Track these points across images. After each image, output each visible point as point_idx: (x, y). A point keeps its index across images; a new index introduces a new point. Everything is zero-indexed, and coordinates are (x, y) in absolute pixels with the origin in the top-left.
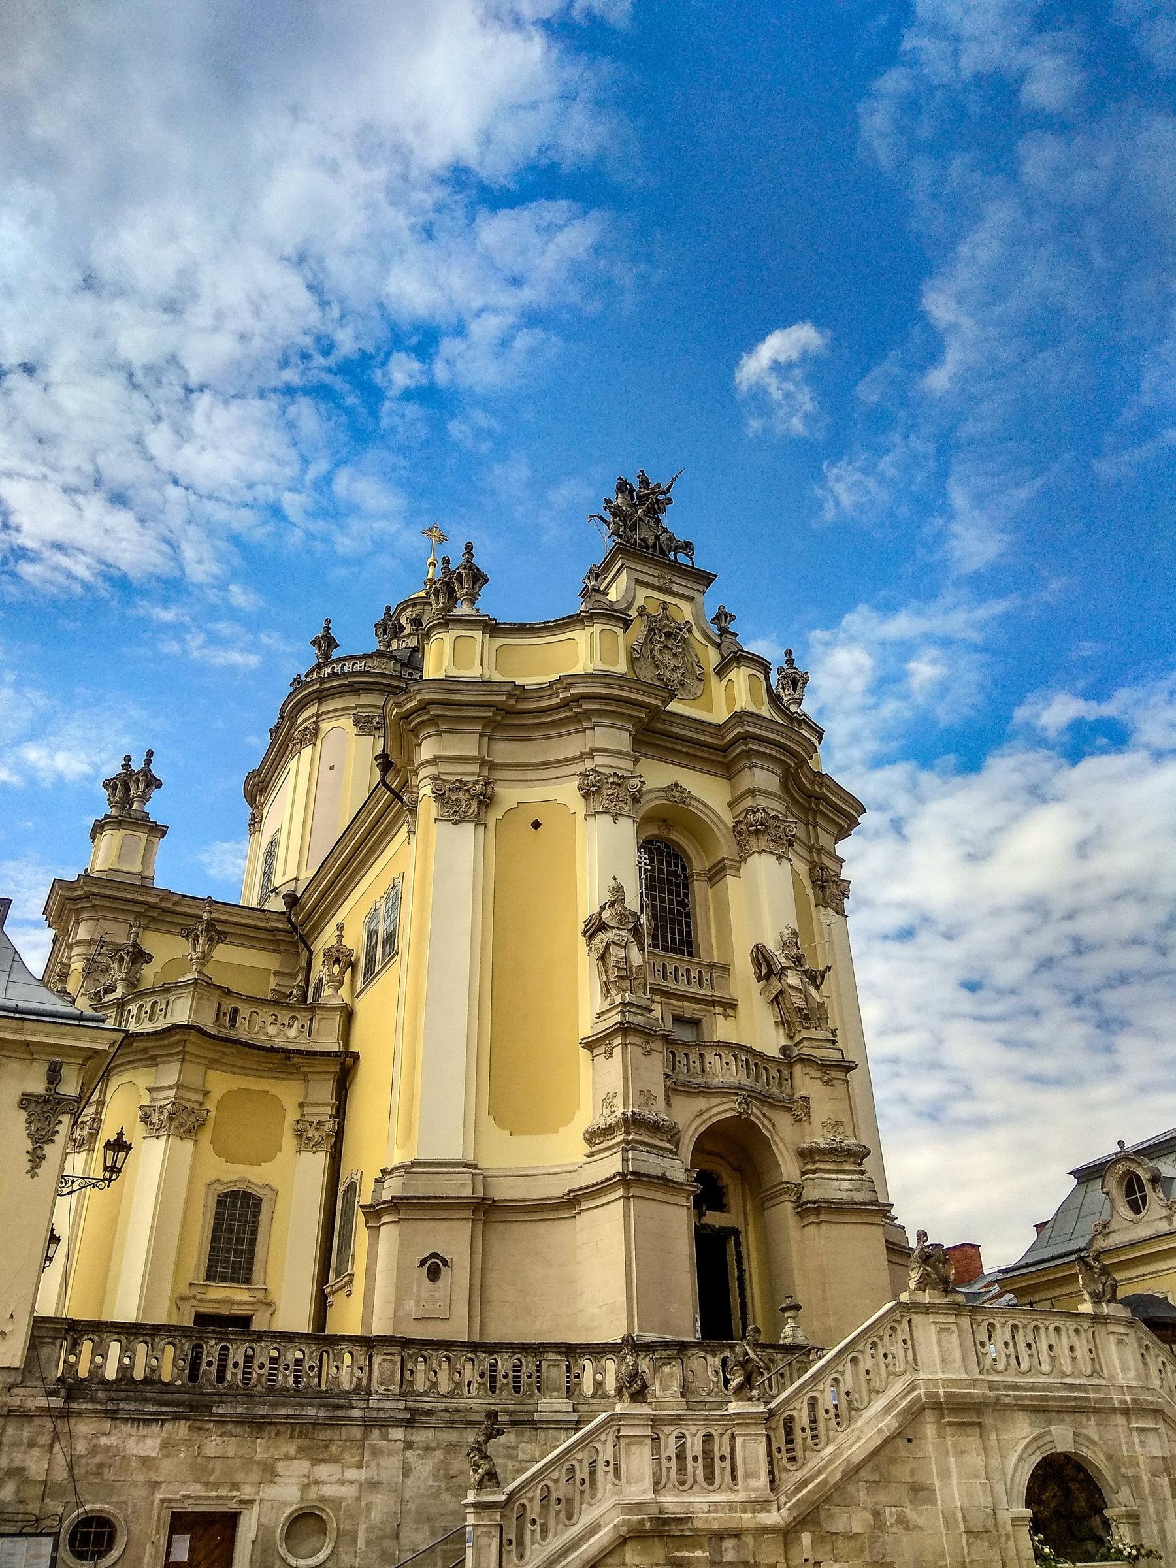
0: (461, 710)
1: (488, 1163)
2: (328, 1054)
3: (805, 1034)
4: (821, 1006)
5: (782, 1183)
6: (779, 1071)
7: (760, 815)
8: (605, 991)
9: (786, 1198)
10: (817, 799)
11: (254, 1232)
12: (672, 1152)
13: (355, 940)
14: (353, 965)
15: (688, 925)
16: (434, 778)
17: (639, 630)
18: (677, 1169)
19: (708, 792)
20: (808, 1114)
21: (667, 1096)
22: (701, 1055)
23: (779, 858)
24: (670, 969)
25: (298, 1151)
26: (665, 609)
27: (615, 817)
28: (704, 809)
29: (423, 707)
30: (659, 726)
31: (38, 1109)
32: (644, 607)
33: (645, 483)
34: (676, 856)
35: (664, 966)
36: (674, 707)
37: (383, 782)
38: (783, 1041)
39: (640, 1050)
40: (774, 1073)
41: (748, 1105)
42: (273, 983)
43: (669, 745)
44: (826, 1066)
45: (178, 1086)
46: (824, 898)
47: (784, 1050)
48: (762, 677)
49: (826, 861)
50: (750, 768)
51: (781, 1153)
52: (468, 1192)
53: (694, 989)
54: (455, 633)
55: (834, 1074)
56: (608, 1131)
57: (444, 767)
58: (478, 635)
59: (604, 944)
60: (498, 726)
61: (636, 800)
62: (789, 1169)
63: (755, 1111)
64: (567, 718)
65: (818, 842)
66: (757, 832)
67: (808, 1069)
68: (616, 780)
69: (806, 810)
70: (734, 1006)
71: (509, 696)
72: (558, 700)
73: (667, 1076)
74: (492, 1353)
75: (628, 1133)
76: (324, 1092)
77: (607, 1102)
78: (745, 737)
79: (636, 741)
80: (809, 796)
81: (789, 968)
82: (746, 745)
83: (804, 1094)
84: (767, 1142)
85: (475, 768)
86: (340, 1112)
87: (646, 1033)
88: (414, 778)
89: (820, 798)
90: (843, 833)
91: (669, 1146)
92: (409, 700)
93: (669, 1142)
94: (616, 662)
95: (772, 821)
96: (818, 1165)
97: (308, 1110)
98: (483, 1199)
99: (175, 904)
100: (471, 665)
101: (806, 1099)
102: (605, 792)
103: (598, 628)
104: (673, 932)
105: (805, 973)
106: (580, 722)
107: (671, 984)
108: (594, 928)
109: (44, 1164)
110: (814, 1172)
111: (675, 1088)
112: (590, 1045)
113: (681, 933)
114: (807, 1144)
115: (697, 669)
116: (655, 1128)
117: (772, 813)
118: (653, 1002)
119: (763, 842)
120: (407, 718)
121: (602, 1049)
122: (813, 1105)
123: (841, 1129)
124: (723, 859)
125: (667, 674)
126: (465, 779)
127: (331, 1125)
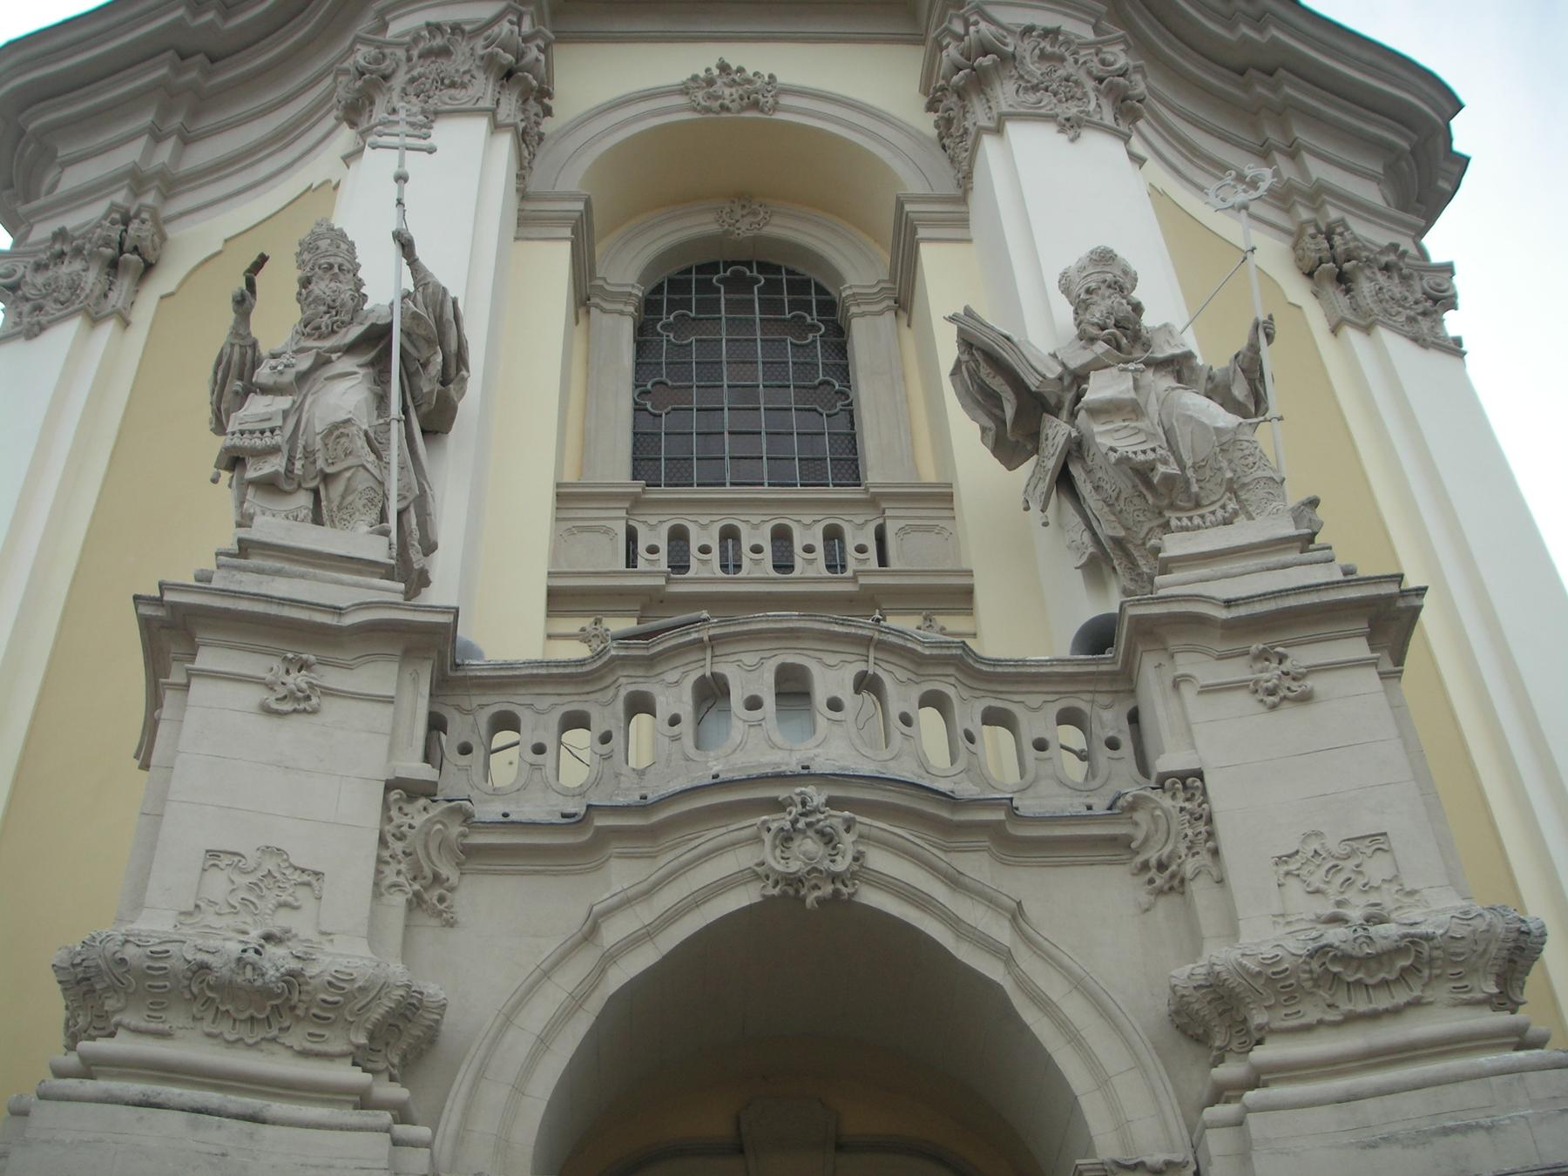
3: (1174, 545)
10: (1271, 74)
12: (364, 1100)
23: (1072, 126)
34: (800, 285)
39: (256, 695)
41: (828, 839)
44: (1269, 626)
46: (1355, 309)
47: (1097, 637)
51: (1075, 1039)
55: (1302, 657)
60: (203, 102)
66: (979, 82)
67: (1186, 663)
68: (439, 41)
69: (1250, 114)
83: (1169, 760)
91: (354, 1076)
93: (358, 1058)
101: (1190, 781)
102: (399, 81)
110: (1256, 1080)
114: (1185, 972)
122: (1221, 795)
123: (1377, 869)
124: (900, 205)
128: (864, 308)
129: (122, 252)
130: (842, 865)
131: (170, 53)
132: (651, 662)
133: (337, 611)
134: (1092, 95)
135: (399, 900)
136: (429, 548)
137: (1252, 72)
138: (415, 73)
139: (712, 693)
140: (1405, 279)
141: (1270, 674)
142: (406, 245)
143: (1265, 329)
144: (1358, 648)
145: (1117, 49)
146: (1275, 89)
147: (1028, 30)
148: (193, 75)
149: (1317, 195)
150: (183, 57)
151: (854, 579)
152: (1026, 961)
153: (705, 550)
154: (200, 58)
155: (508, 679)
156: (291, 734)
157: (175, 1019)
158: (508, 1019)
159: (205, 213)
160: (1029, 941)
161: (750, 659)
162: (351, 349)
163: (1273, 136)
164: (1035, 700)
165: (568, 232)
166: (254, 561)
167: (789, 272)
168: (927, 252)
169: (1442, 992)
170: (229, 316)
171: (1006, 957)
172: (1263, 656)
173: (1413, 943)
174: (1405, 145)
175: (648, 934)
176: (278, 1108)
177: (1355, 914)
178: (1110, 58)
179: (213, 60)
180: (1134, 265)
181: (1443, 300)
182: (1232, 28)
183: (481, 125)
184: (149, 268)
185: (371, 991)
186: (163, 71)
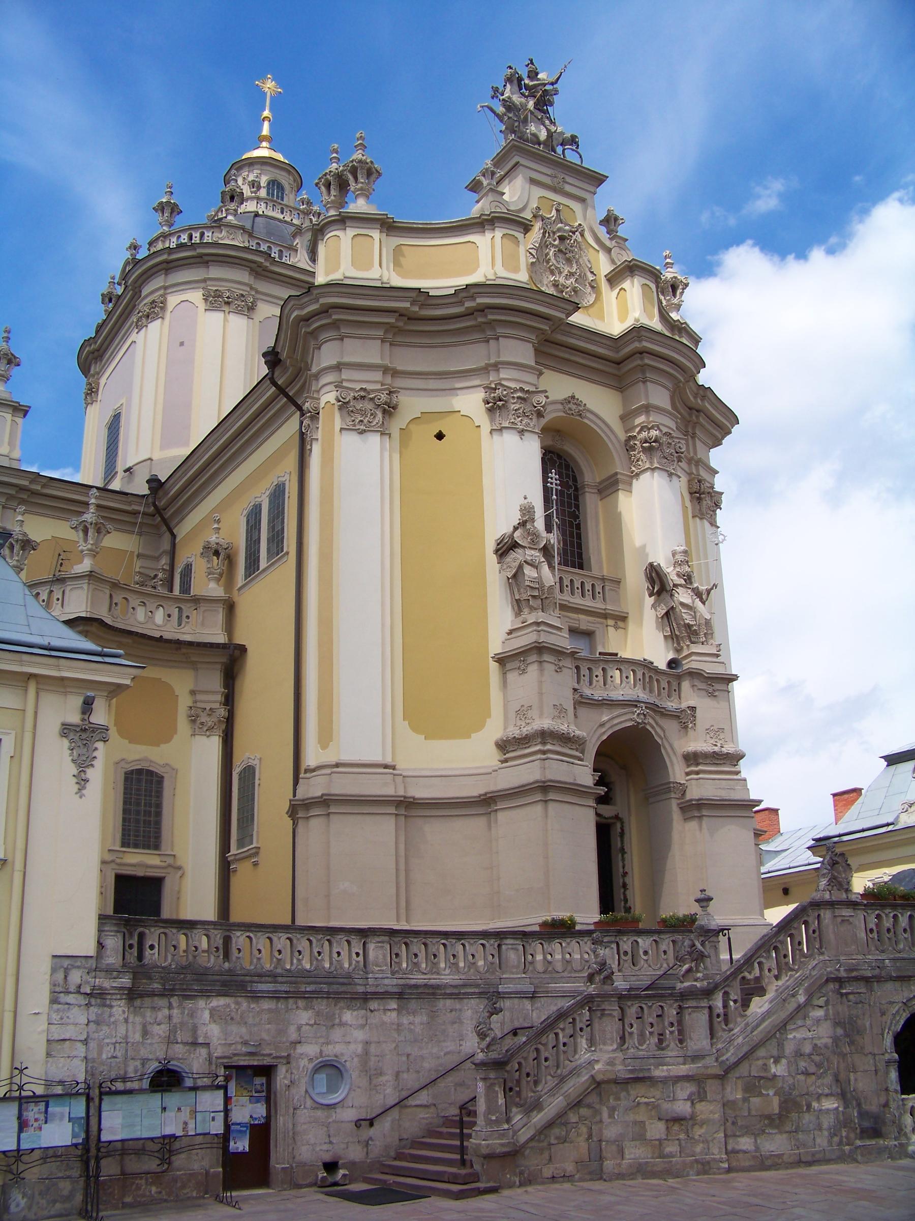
1: (403, 765)
2: (218, 646)
4: (708, 623)
5: (670, 783)
6: (669, 682)
7: (654, 433)
8: (516, 608)
9: (673, 795)
10: (697, 411)
11: (159, 806)
13: (234, 531)
14: (230, 560)
15: (579, 536)
16: (338, 386)
17: (536, 234)
18: (585, 775)
19: (600, 403)
20: (694, 721)
21: (575, 708)
22: (603, 669)
23: (670, 475)
24: (566, 582)
25: (193, 735)
28: (598, 422)
29: (326, 310)
31: (77, 738)
32: (538, 208)
34: (568, 467)
36: (577, 318)
37: (270, 378)
39: (553, 667)
40: (664, 684)
41: (645, 715)
42: (138, 565)
43: (567, 356)
46: (700, 510)
47: (672, 664)
48: (653, 286)
49: (703, 474)
50: (644, 382)
52: (389, 791)
53: (587, 602)
54: (351, 232)
56: (523, 741)
57: (346, 374)
58: (376, 234)
59: (517, 564)
60: (400, 331)
61: (540, 415)
63: (651, 721)
65: (695, 453)
67: (697, 682)
73: (575, 690)
74: (460, 939)
75: (544, 743)
76: (214, 682)
77: (522, 713)
78: (641, 352)
79: (538, 352)
81: (681, 585)
82: (642, 359)
84: (658, 746)
85: (378, 376)
86: (229, 700)
88: (314, 382)
90: (717, 443)
92: (311, 302)
93: (577, 750)
96: (700, 767)
97: (199, 697)
98: (405, 797)
99: (44, 486)
101: (693, 709)
105: (693, 590)
108: (506, 548)
109: (88, 785)
110: (697, 773)
111: (582, 702)
112: (502, 660)
116: (565, 739)
117: (665, 430)
120: (308, 320)
121: (516, 664)
122: (699, 713)
125: (562, 280)
126: (369, 387)
127: (222, 712)
128: (590, 490)
138: (517, 406)
143: (715, 586)
151: (605, 609)
154: (406, 318)
159: (408, 391)
169: (728, 762)
170: (512, 529)
175: (611, 727)
181: (717, 505)
182: (695, 398)
186: (393, 321)
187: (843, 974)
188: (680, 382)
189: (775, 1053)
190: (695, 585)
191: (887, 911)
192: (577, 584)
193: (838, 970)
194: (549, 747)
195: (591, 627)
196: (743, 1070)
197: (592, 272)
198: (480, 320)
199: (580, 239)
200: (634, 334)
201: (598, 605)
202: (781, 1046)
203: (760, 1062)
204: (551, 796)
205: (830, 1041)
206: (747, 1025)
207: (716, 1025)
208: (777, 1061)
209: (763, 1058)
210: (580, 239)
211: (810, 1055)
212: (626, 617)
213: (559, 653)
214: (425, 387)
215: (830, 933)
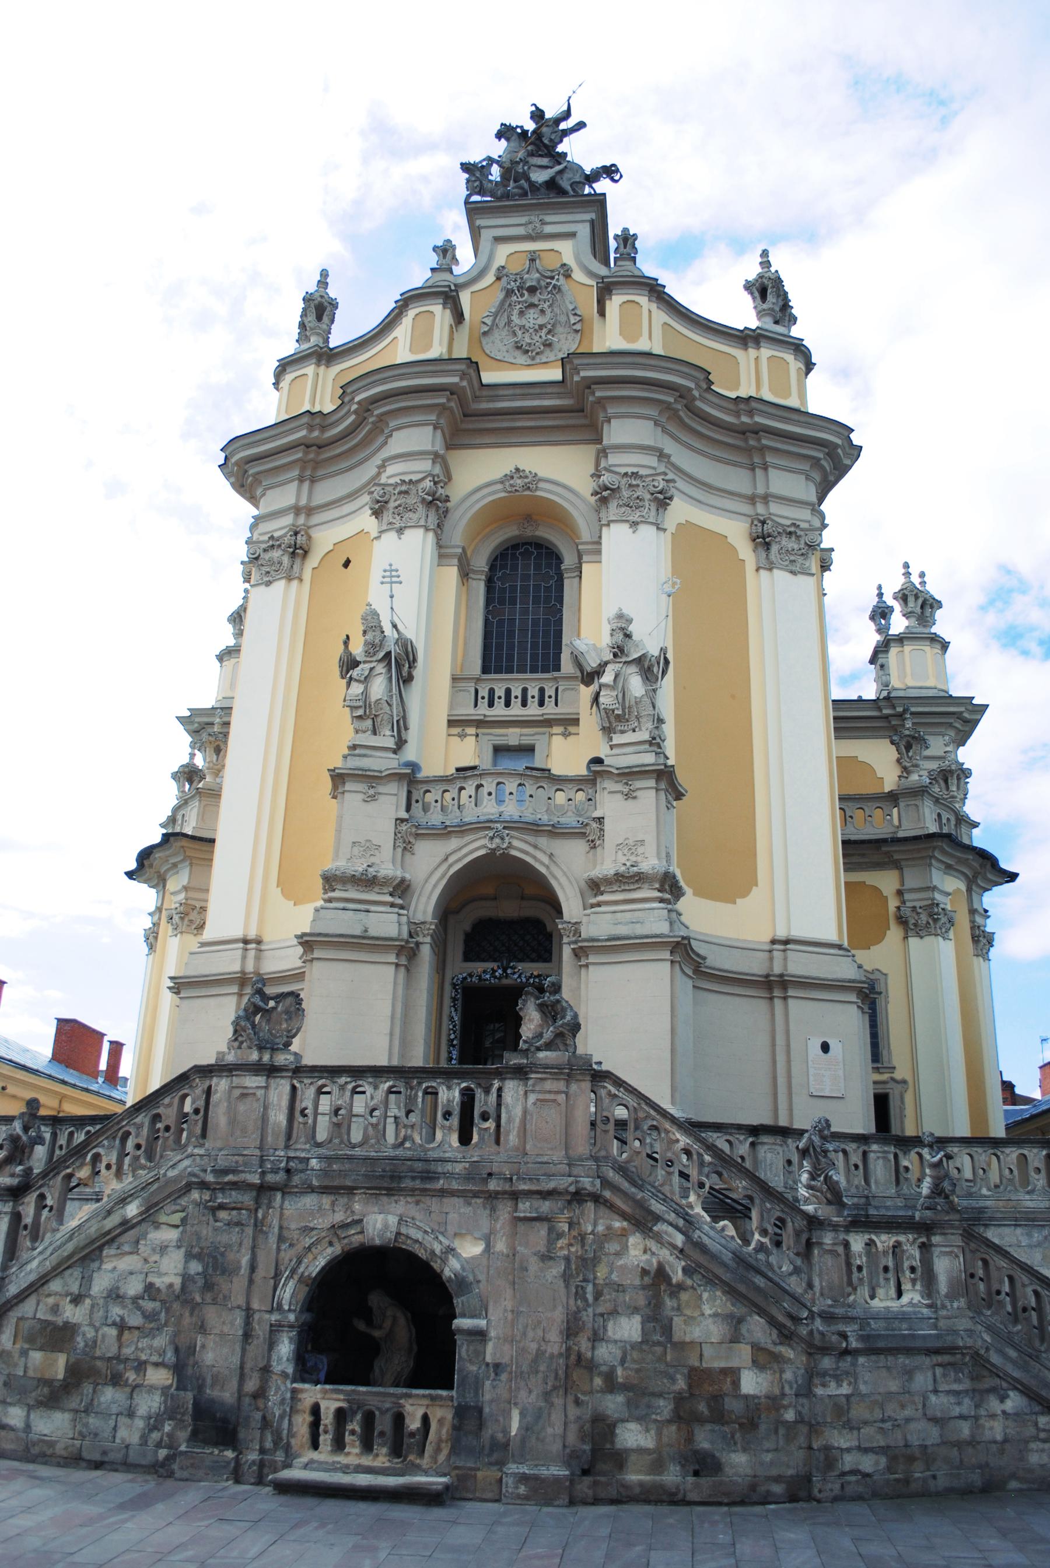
0: (275, 460)
7: (606, 478)
10: (756, 433)
12: (392, 905)
20: (602, 837)
23: (634, 524)
24: (500, 692)
26: (532, 260)
27: (400, 531)
28: (559, 490)
30: (484, 406)
33: (538, 115)
35: (492, 692)
36: (487, 377)
38: (602, 751)
39: (361, 796)
41: (502, 839)
43: (506, 424)
44: (629, 775)
45: (185, 888)
48: (643, 300)
51: (562, 888)
52: (236, 967)
53: (533, 710)
54: (288, 377)
55: (638, 784)
58: (310, 370)
60: (317, 464)
61: (437, 504)
62: (571, 907)
64: (370, 432)
66: (604, 501)
68: (404, 488)
69: (748, 451)
70: (576, 722)
71: (311, 428)
72: (353, 417)
80: (743, 432)
82: (593, 393)
87: (371, 779)
89: (757, 431)
91: (389, 899)
94: (428, 347)
95: (624, 481)
96: (600, 898)
98: (243, 972)
100: (302, 404)
101: (600, 820)
102: (392, 504)
103: (411, 313)
104: (535, 645)
106: (383, 431)
107: (499, 711)
110: (599, 905)
113: (546, 646)
115: (573, 320)
116: (367, 881)
117: (623, 470)
118: (465, 735)
119: (613, 510)
122: (607, 826)
123: (640, 850)
126: (276, 535)
128: (569, 575)
129: (296, 549)
130: (505, 846)
131: (302, 447)
132: (465, 778)
133: (381, 772)
134: (647, 504)
135: (400, 850)
136: (406, 729)
137: (748, 434)
138: (398, 502)
139: (479, 786)
140: (798, 537)
141: (626, 790)
142: (395, 626)
144: (652, 783)
145: (660, 478)
146: (759, 440)
147: (626, 474)
148: (311, 456)
149: (766, 498)
150: (308, 446)
151: (543, 715)
152: (553, 868)
153: (500, 698)
155: (427, 781)
156: (371, 807)
157: (349, 886)
158: (426, 881)
160: (555, 862)
161: (490, 780)
162: (380, 661)
163: (756, 460)
164: (570, 786)
165: (455, 561)
166: (357, 752)
167: (547, 548)
168: (584, 566)
169: (646, 886)
170: (343, 647)
171: (548, 867)
172: (626, 784)
173: (639, 873)
174: (821, 455)
176: (373, 908)
177: (628, 864)
178: (656, 484)
179: (320, 447)
180: (632, 615)
183: (421, 531)
184: (306, 553)
185: (394, 878)
186: (300, 455)
187: (210, 1178)
188: (670, 403)
189: (75, 1288)
190: (636, 656)
191: (342, 1080)
192: (516, 691)
193: (206, 1171)
194: (337, 894)
195: (526, 741)
196: (28, 1308)
197: (575, 314)
198: (371, 420)
199: (562, 281)
200: (568, 367)
201: (550, 709)
202: (86, 1281)
203: (51, 1301)
204: (317, 954)
205: (177, 1281)
206: (51, 1244)
207: (20, 1239)
208: (77, 1300)
209: (56, 1294)
210: (562, 281)
211: (135, 1299)
212: (578, 719)
213: (371, 779)
214: (337, 516)
215: (219, 1117)
